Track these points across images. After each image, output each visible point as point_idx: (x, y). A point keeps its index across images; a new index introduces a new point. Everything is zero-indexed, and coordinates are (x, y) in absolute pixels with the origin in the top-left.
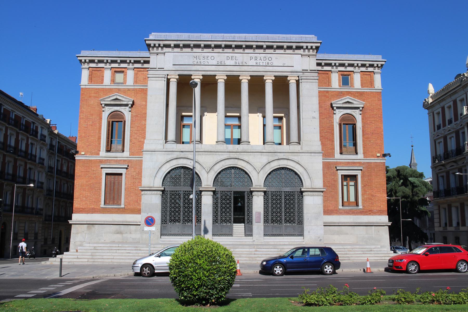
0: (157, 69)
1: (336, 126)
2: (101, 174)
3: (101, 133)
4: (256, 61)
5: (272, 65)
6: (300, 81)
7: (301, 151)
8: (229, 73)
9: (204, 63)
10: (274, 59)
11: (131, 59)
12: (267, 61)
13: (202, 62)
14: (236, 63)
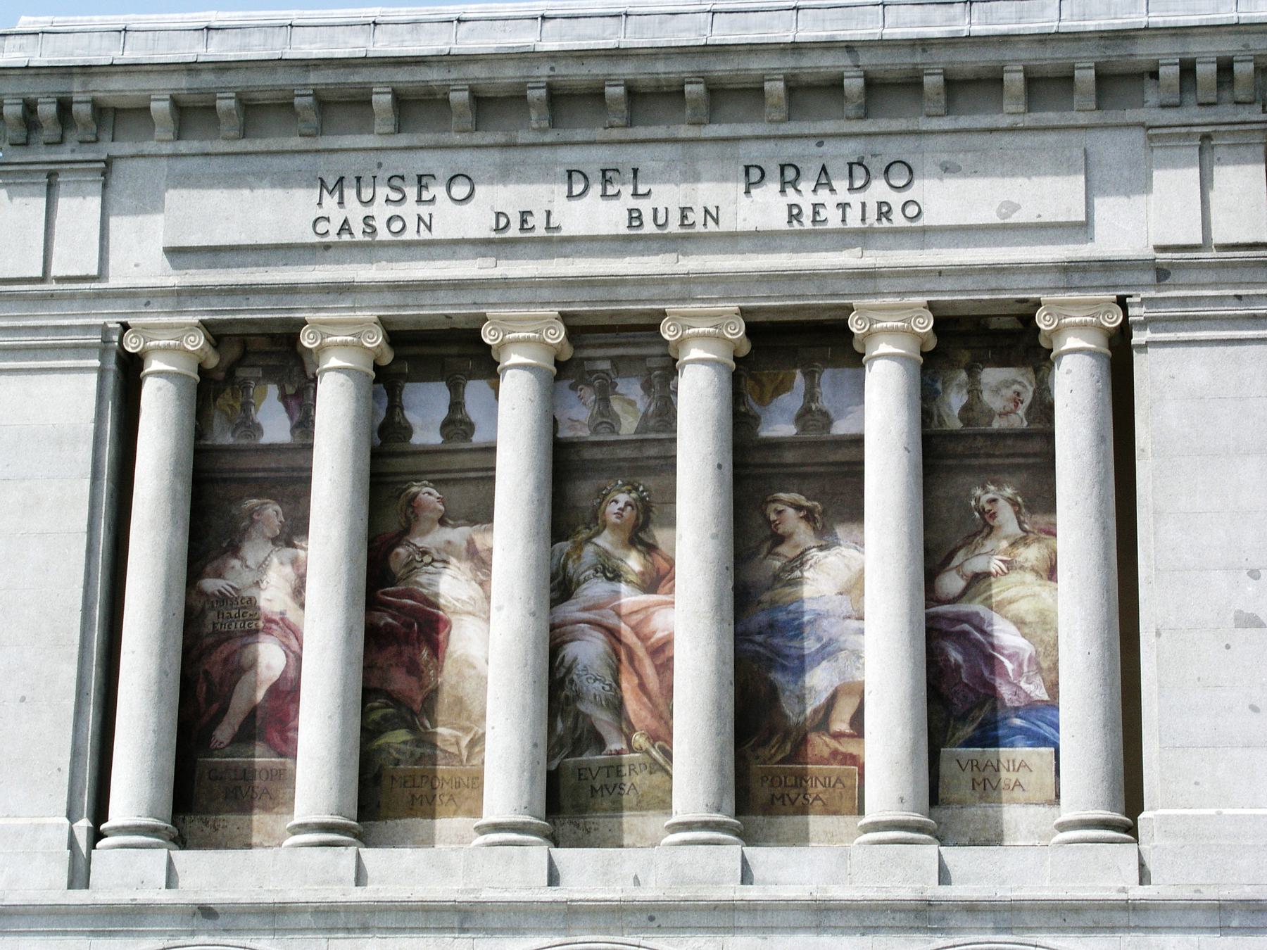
0: (53, 286)
5: (919, 223)
9: (397, 226)
13: (380, 224)
14: (635, 217)
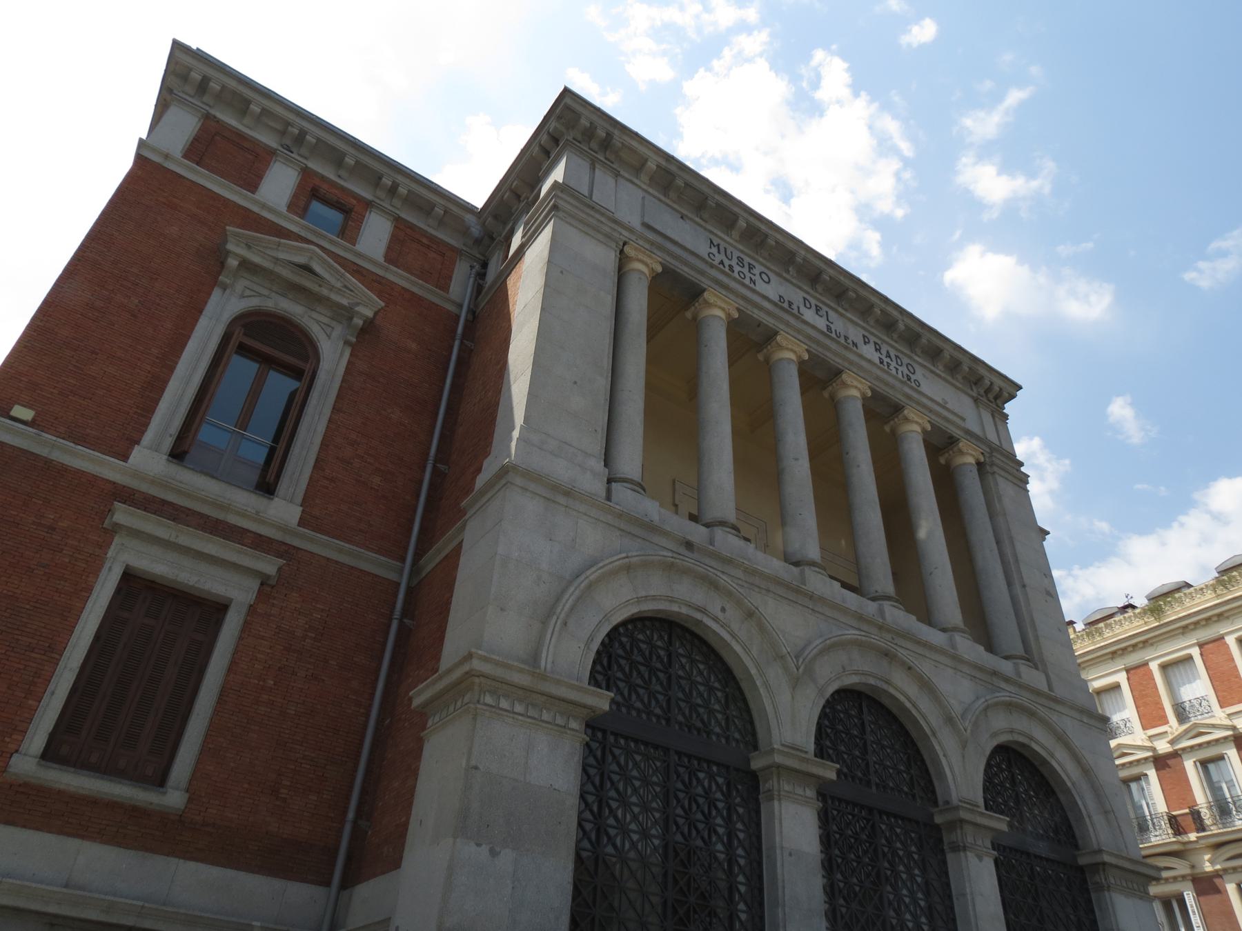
2: (94, 566)
3: (171, 369)
11: (400, 179)
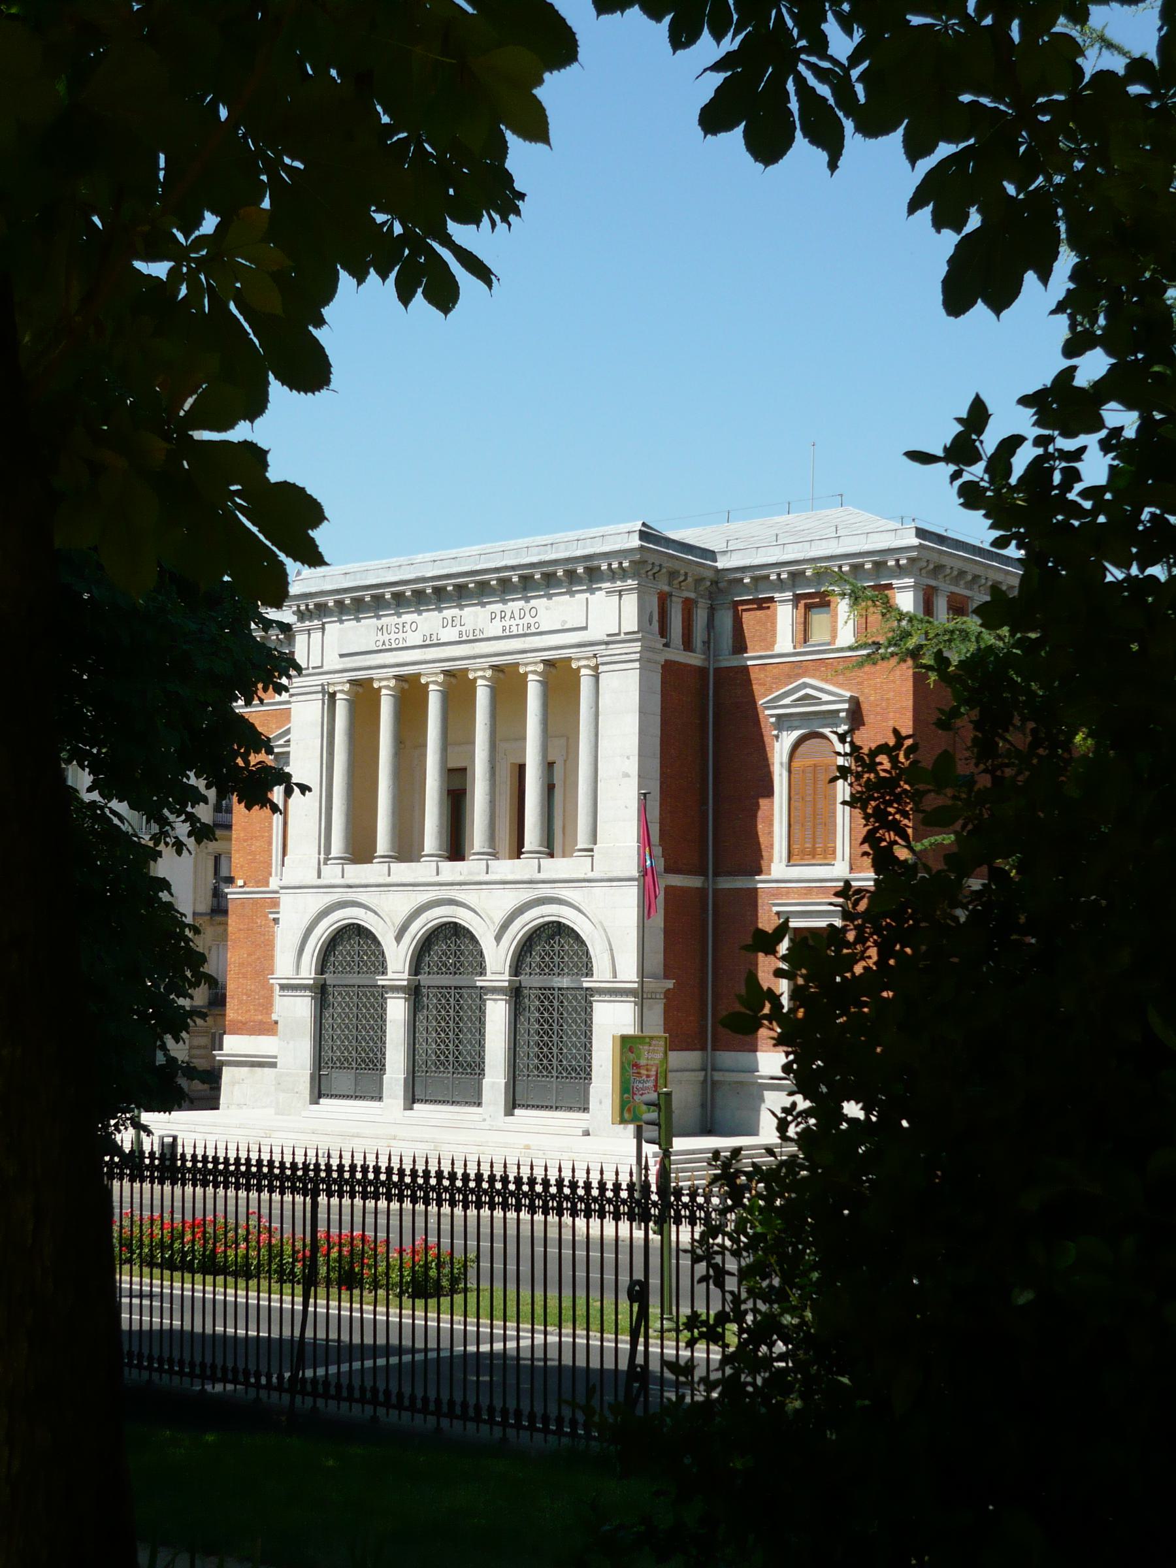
1: (781, 775)
4: (504, 623)
6: (601, 668)
7: (591, 875)
8: (447, 666)
10: (541, 612)
12: (528, 619)
13: (392, 641)
14: (460, 633)
